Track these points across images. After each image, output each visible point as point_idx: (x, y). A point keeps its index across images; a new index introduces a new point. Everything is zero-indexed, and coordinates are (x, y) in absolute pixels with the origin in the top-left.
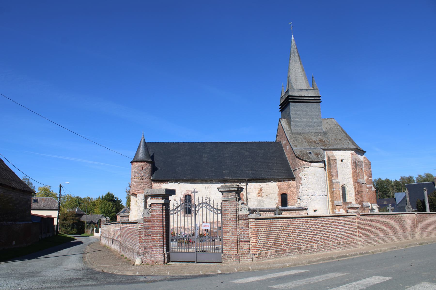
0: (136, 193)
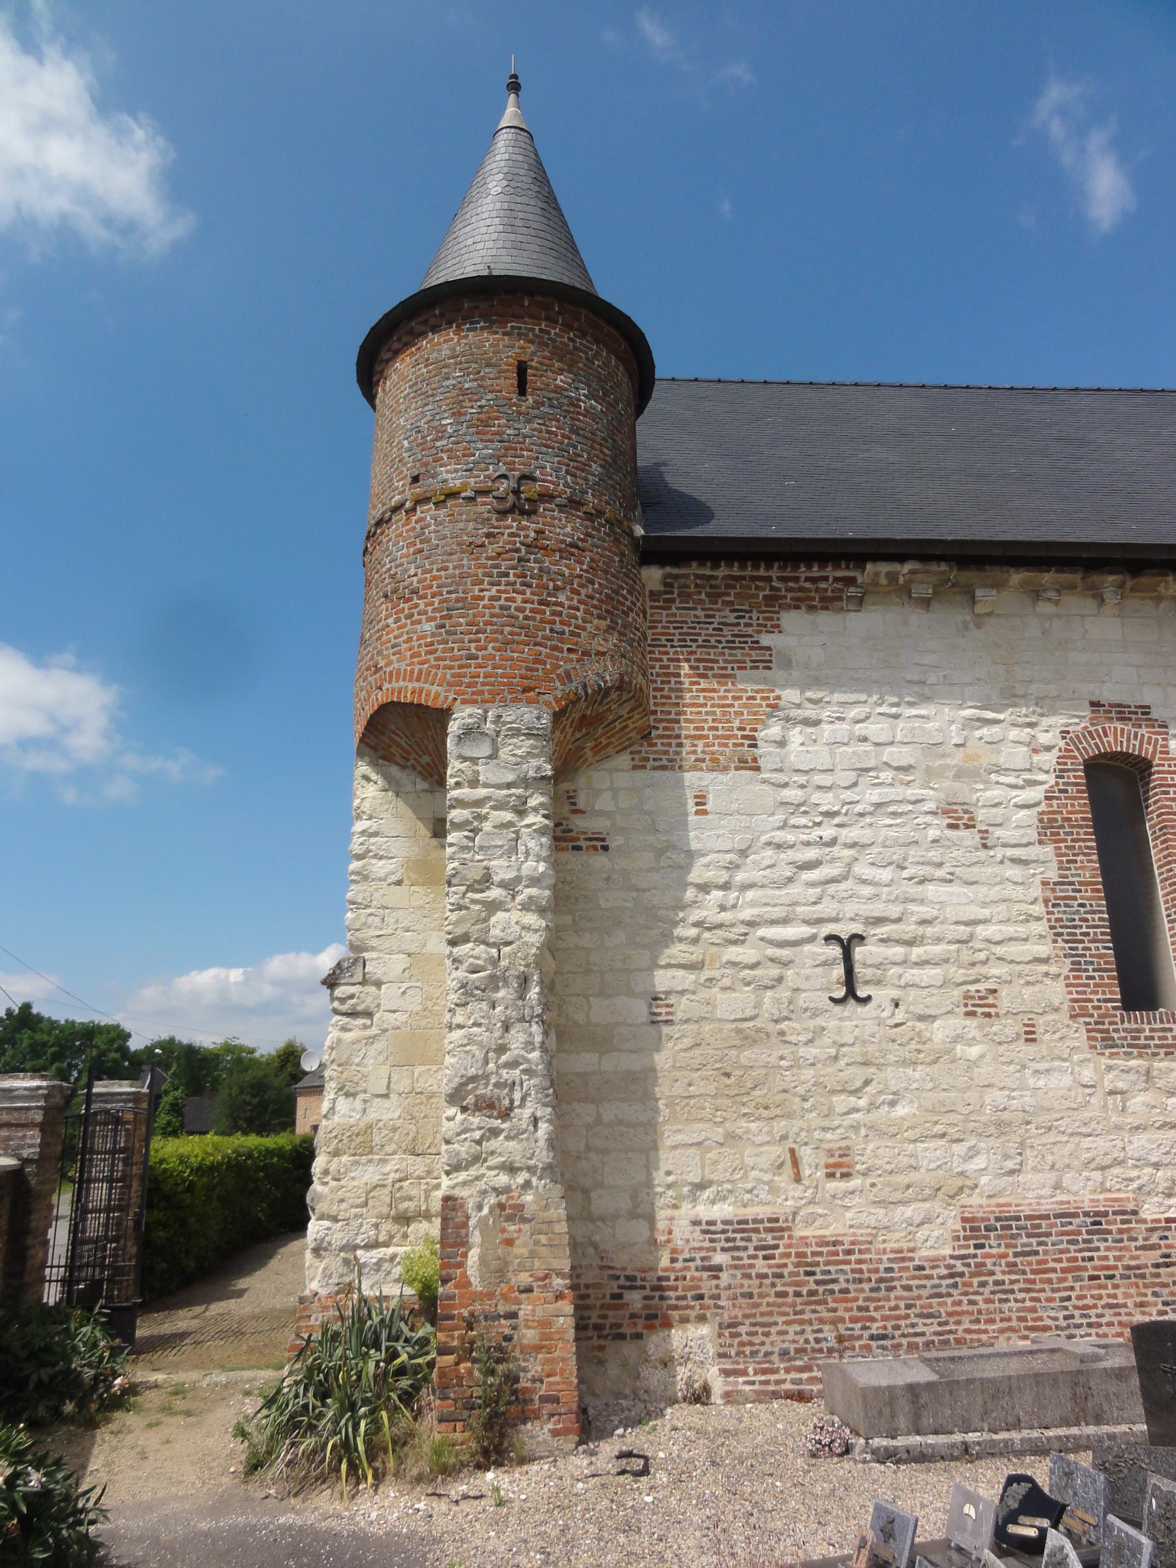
0: (434, 693)
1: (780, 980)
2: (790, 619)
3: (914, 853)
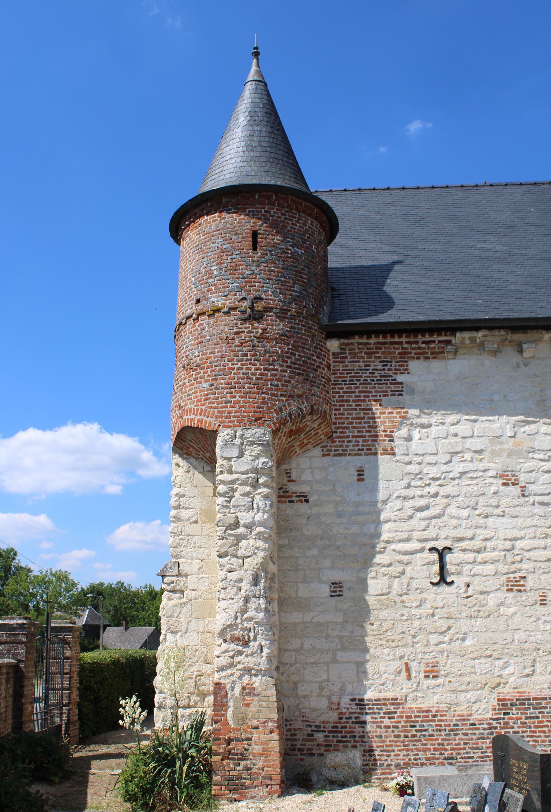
1: (403, 573)
2: (414, 365)
3: (482, 501)
